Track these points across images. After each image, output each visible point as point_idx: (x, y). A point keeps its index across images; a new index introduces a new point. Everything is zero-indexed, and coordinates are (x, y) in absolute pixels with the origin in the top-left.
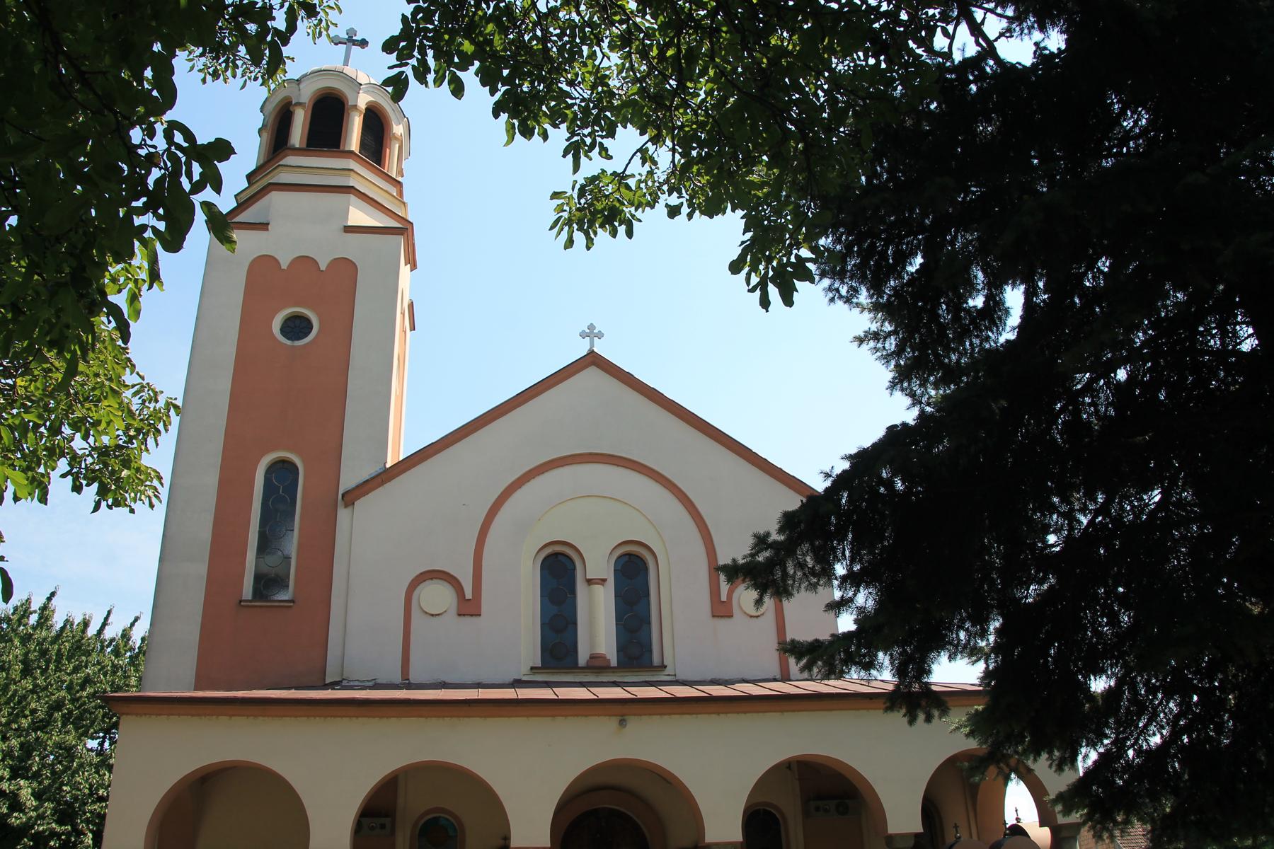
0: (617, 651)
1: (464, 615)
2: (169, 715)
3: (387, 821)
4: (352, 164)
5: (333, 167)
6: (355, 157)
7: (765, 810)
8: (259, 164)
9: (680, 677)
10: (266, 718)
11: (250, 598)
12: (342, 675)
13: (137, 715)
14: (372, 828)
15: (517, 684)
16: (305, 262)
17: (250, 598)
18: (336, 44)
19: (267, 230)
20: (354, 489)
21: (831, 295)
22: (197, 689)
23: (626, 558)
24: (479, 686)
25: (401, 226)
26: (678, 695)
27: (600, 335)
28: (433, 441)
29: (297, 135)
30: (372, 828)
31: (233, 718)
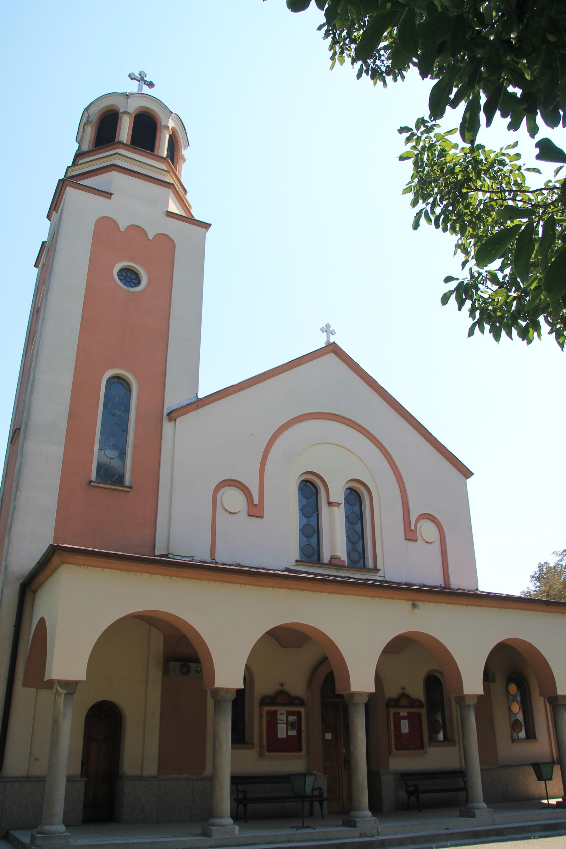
1: (252, 516)
2: (103, 568)
6: (167, 164)
10: (179, 578)
13: (77, 564)
16: (136, 229)
18: (132, 79)
19: (110, 198)
20: (179, 409)
27: (333, 333)
28: (234, 384)
31: (154, 575)
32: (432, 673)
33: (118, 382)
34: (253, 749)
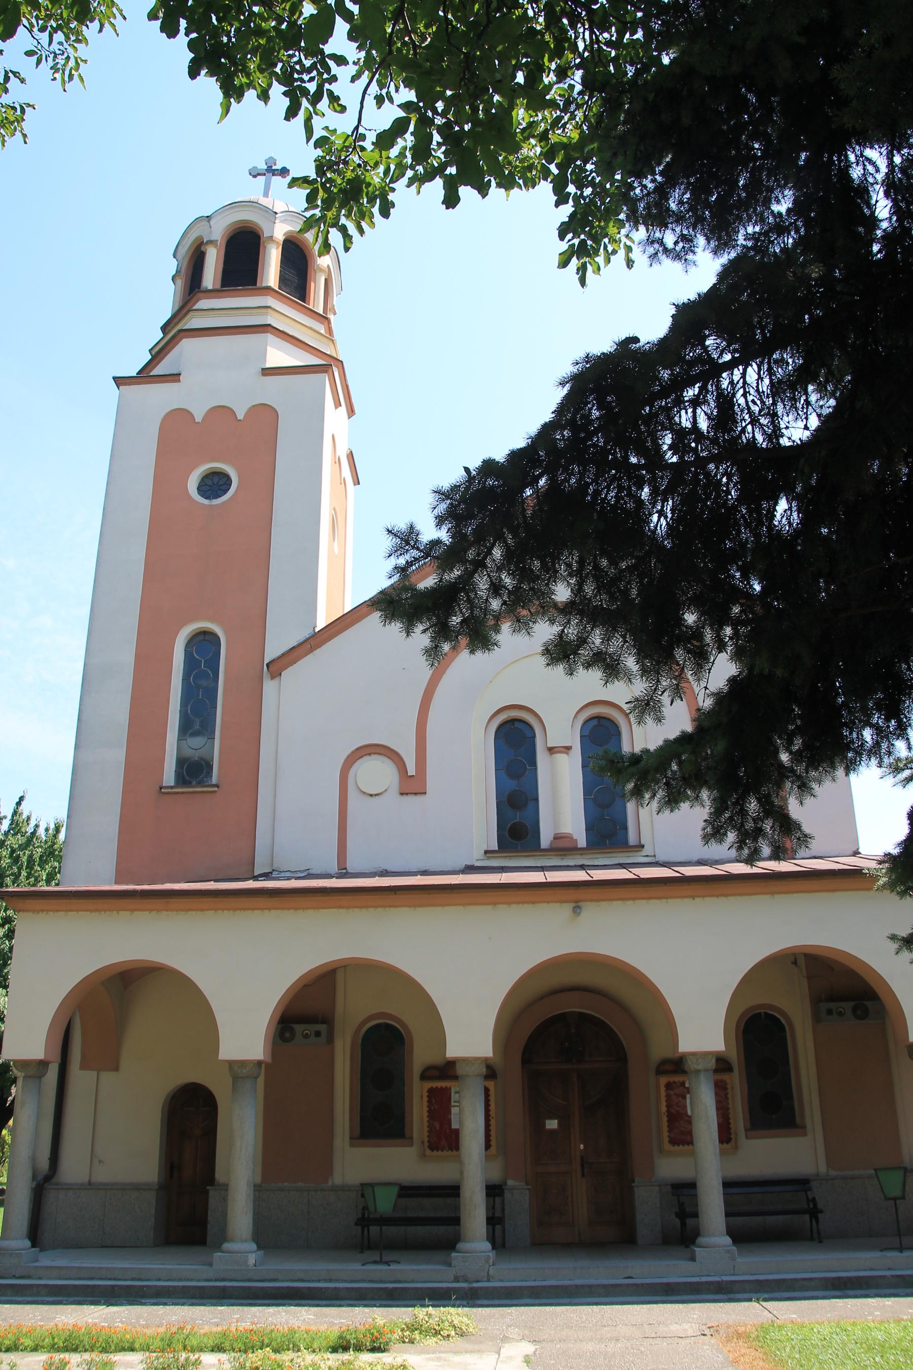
0: (586, 830)
1: (407, 794)
2: (67, 911)
3: (323, 1028)
4: (270, 301)
5: (248, 306)
6: (275, 294)
7: (765, 1013)
8: (174, 312)
9: (661, 858)
10: (170, 913)
11: (172, 784)
12: (272, 865)
13: (34, 911)
14: (306, 1036)
15: (470, 869)
16: (221, 412)
17: (172, 784)
18: (255, 176)
19: (179, 381)
20: (279, 658)
21: (651, 250)
22: (116, 883)
23: (595, 722)
24: (425, 873)
25: (324, 363)
26: (642, 876)
29: (211, 276)
30: (306, 1036)
32: (762, 1011)
33: (204, 640)
34: (412, 1145)
